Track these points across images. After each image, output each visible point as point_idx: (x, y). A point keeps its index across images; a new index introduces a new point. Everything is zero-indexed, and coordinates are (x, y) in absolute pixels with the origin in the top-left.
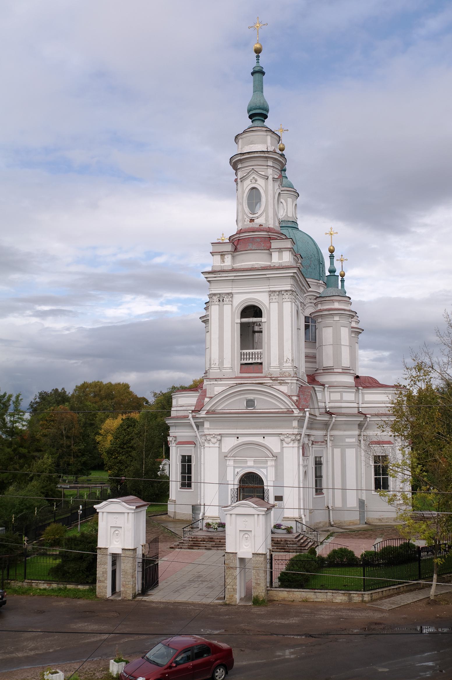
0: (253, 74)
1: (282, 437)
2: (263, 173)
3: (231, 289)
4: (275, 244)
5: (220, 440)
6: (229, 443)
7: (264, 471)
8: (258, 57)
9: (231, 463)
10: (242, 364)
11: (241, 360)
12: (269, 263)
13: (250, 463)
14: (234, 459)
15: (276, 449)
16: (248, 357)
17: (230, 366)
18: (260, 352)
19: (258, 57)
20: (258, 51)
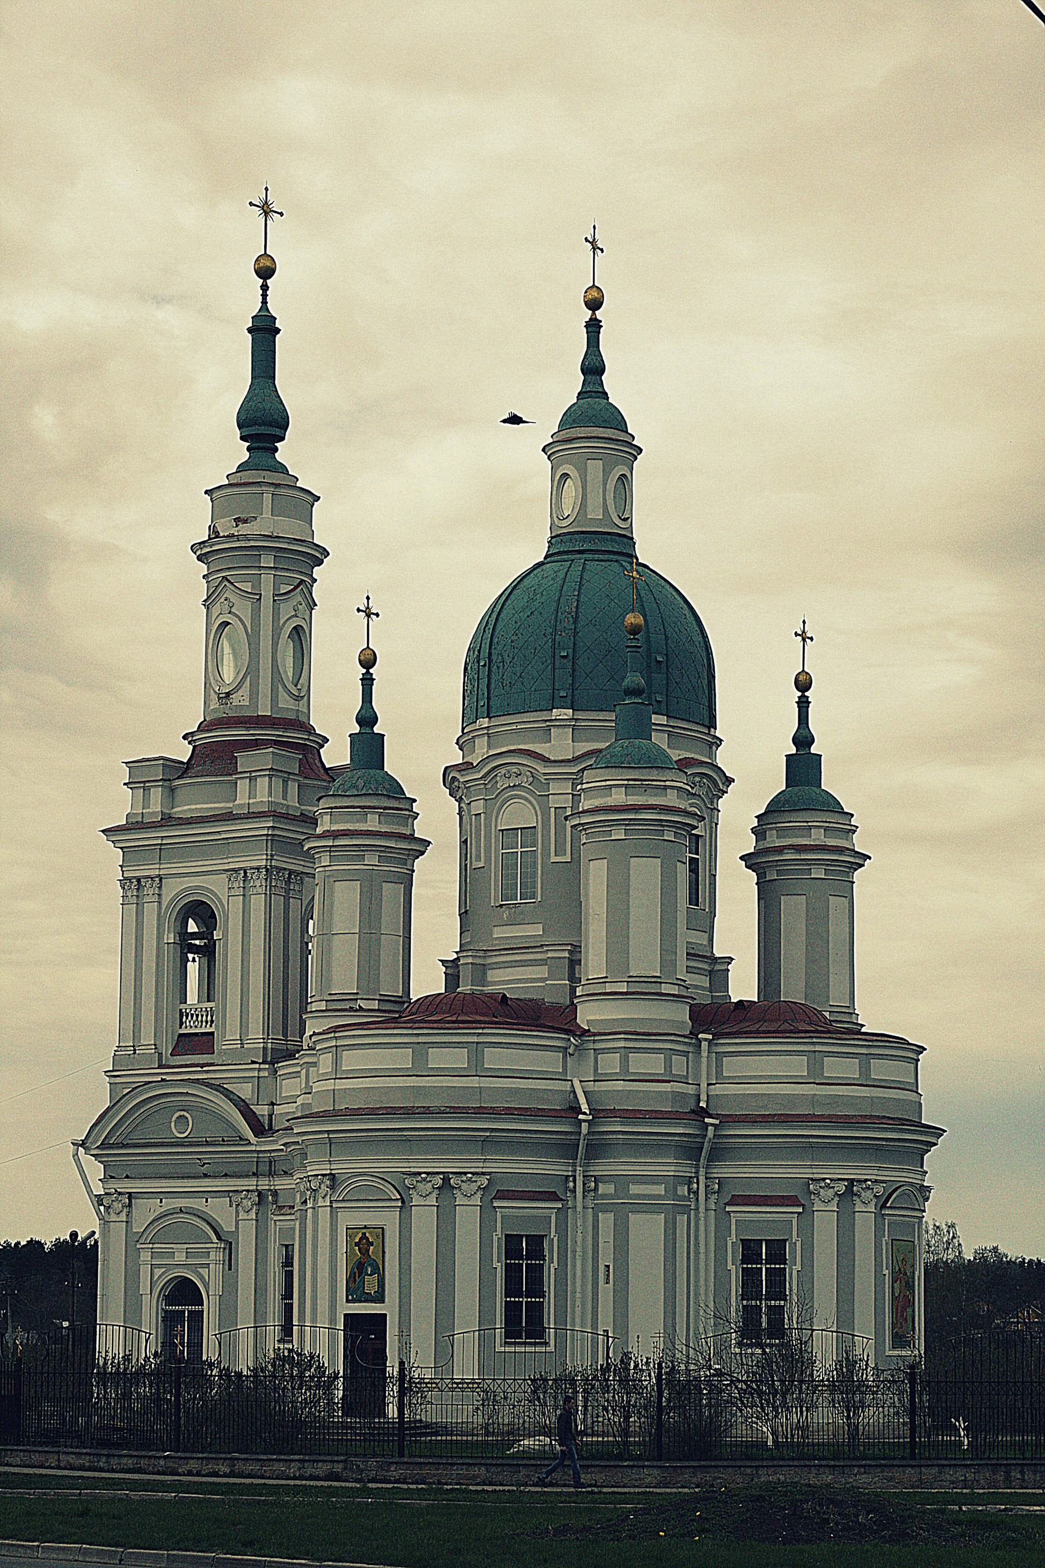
0: (250, 330)
1: (236, 1198)
2: (247, 587)
3: (157, 866)
4: (245, 761)
5: (130, 1205)
6: (146, 1212)
7: (204, 1272)
8: (265, 288)
9: (145, 1256)
10: (180, 1035)
11: (181, 1028)
12: (231, 805)
13: (180, 1258)
14: (152, 1248)
15: (228, 1226)
16: (209, 1018)
17: (153, 1042)
18: (211, 1008)
19: (265, 288)
20: (265, 271)
